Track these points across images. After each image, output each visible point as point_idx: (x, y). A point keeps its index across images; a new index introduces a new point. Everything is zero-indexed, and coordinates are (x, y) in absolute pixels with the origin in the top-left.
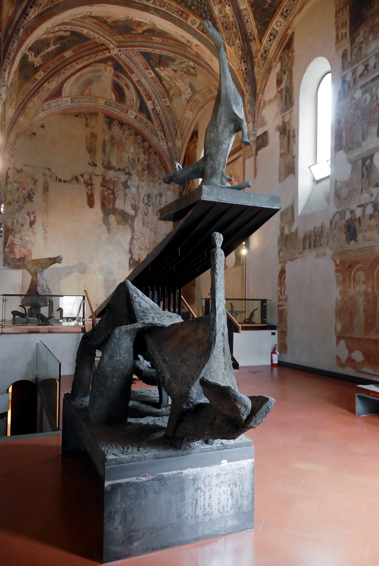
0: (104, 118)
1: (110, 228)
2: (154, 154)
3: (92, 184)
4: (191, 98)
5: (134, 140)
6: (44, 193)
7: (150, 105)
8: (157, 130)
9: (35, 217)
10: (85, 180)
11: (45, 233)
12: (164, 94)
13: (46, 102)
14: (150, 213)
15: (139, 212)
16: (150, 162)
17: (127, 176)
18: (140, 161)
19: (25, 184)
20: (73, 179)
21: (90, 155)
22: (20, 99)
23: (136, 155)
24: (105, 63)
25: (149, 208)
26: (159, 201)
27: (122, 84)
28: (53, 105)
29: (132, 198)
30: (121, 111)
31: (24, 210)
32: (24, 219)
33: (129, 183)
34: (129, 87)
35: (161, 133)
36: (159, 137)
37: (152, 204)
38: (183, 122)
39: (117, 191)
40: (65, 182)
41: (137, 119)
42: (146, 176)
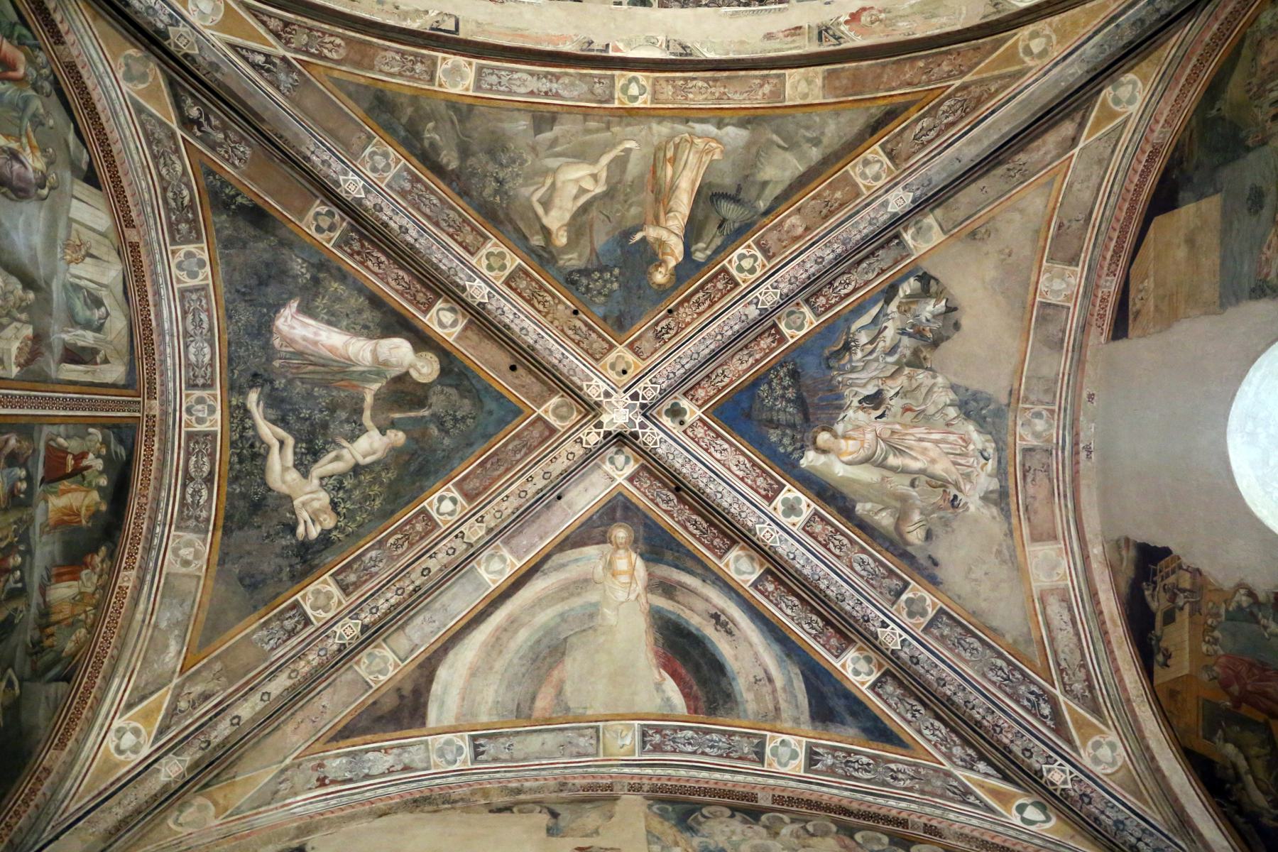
0: (650, 807)
4: (1001, 472)
7: (857, 673)
8: (948, 766)
12: (891, 572)
13: (341, 744)
22: (206, 697)
24: (603, 539)
27: (697, 621)
30: (728, 757)
34: (730, 625)
36: (977, 798)
38: (1048, 625)
41: (819, 766)
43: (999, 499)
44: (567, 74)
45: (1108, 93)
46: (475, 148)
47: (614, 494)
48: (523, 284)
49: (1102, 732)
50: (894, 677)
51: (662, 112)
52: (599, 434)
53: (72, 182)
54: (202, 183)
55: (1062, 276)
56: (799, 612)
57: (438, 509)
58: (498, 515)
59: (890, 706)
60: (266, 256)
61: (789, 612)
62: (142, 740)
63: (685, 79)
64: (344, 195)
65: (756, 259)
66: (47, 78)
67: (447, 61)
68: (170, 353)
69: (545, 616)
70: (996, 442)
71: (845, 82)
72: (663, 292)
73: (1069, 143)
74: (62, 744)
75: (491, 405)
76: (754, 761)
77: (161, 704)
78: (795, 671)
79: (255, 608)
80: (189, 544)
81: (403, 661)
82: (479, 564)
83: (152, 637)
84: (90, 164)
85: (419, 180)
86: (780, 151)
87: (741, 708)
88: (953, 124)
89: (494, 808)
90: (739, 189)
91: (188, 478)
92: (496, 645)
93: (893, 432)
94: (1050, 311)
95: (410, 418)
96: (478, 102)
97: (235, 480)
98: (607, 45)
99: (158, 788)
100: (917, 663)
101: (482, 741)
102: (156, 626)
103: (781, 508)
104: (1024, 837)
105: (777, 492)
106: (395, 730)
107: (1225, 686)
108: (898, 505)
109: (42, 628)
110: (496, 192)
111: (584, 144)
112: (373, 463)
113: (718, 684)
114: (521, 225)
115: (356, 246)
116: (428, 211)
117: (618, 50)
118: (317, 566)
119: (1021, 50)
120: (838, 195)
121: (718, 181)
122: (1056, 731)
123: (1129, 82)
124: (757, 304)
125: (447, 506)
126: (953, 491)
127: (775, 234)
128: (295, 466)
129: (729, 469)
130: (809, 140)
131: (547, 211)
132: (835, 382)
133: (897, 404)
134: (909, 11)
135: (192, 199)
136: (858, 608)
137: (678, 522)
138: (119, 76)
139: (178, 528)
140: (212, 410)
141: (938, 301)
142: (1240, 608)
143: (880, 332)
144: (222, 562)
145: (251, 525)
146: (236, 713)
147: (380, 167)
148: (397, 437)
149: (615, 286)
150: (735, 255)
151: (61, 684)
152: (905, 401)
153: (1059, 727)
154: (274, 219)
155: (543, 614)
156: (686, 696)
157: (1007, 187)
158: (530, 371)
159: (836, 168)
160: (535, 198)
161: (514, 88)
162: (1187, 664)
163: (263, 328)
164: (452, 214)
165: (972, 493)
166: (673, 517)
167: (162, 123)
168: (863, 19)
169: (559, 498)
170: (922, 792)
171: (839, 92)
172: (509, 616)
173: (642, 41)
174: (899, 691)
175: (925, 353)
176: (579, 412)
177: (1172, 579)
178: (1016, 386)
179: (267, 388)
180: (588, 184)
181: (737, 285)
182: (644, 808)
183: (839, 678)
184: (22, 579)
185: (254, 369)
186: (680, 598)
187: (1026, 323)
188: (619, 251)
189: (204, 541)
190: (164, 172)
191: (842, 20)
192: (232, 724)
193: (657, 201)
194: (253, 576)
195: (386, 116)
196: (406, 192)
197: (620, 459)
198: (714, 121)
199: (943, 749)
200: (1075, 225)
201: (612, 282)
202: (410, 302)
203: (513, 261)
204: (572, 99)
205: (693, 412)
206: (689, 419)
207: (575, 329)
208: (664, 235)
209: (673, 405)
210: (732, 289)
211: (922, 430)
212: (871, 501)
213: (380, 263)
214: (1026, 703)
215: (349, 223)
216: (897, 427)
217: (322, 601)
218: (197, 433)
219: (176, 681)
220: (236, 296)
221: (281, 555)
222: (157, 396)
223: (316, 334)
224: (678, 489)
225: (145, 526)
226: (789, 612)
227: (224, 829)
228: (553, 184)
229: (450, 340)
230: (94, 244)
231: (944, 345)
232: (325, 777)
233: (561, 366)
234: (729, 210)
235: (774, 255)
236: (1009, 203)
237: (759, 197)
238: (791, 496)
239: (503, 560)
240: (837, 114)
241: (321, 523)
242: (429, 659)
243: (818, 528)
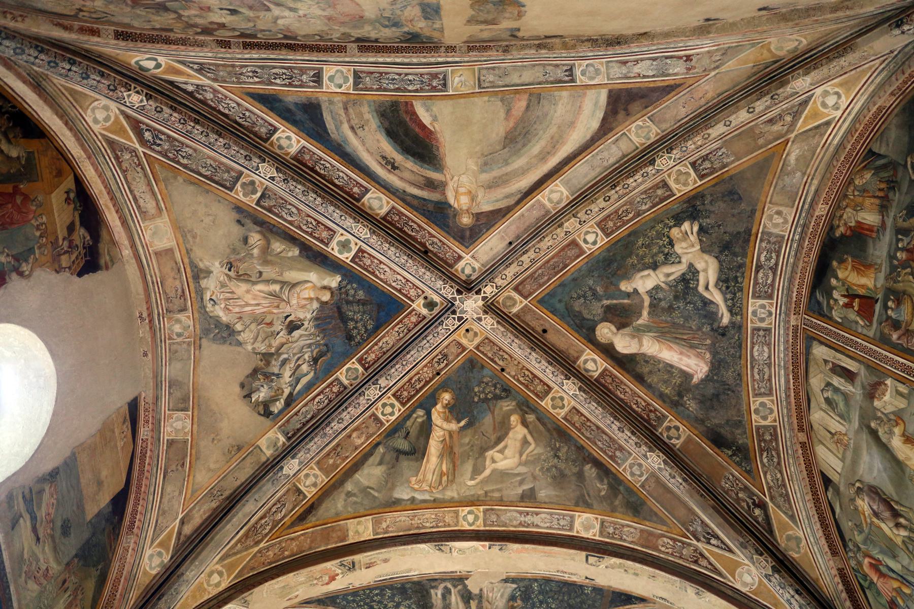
4: (200, 292)
8: (216, 85)
12: (270, 211)
13: (673, 83)
22: (771, 121)
24: (478, 216)
27: (408, 164)
28: (644, 68)
30: (381, 73)
38: (154, 194)
43: (198, 274)
44: (515, 527)
45: (166, 558)
46: (574, 478)
47: (471, 247)
48: (539, 388)
49: (104, 129)
50: (261, 138)
51: (451, 505)
52: (485, 293)
53: (839, 483)
54: (754, 466)
55: (177, 431)
56: (334, 175)
57: (597, 236)
58: (555, 236)
59: (262, 119)
60: (713, 414)
61: (341, 174)
62: (821, 99)
63: (437, 527)
64: (661, 454)
66: (850, 550)
67: (593, 534)
68: (781, 354)
69: (519, 163)
70: (206, 312)
71: (334, 535)
72: (444, 386)
73: (185, 520)
75: (560, 307)
76: (361, 72)
77: (804, 122)
78: (334, 135)
79: (731, 178)
80: (776, 225)
81: (624, 133)
82: (567, 197)
83: (808, 167)
84: (827, 489)
85: (611, 457)
86: (372, 486)
87: (373, 108)
88: (261, 518)
90: (397, 459)
91: (774, 269)
92: (555, 143)
93: (278, 307)
94: (182, 406)
95: (616, 299)
96: (573, 508)
97: (741, 266)
98: (490, 548)
99: (813, 73)
100: (246, 157)
101: (567, 79)
102: (804, 174)
103: (352, 245)
105: (355, 256)
106: (631, 89)
107: (26, 198)
108: (269, 258)
109: (885, 198)
110: (558, 449)
111: (502, 482)
112: (643, 270)
113: (391, 123)
114: (541, 427)
115: (652, 416)
116: (604, 437)
117: (483, 546)
118: (685, 203)
119: (225, 573)
120: (331, 461)
121: (411, 463)
122: (138, 122)
123: (154, 568)
124: (380, 388)
125: (591, 238)
126: (232, 274)
127: (371, 431)
128: (698, 272)
129: (391, 269)
130: (354, 495)
131: (525, 437)
132: (321, 335)
133: (278, 327)
134: (298, 587)
135: (761, 455)
136: (292, 187)
137: (425, 230)
138: (804, 541)
139: (783, 237)
140: (754, 313)
141: (257, 400)
142: (26, 261)
143: (294, 373)
144: (753, 212)
145: (731, 234)
146: (751, 115)
147: (636, 467)
148: (625, 286)
149: (476, 389)
150: (397, 415)
151: (877, 151)
152: (272, 329)
153: (136, 126)
154: (708, 439)
155: (521, 164)
156: (414, 113)
157: (221, 483)
158: (533, 329)
159: (334, 479)
161: (548, 517)
162: (54, 201)
163: (717, 366)
164: (588, 435)
165: (219, 275)
166: (429, 232)
167: (779, 507)
168: (327, 578)
169: (510, 243)
170: (233, 66)
171: (337, 528)
173: (467, 551)
174: (257, 129)
175: (262, 364)
176: (498, 302)
177: (73, 257)
178: (197, 352)
179: (715, 326)
180: (498, 456)
181: (394, 395)
183: (301, 134)
184: (898, 240)
185: (724, 339)
186: (421, 179)
187: (196, 395)
188: (475, 413)
189: (765, 227)
190: (779, 475)
191: (341, 576)
192: (754, 108)
193: (451, 448)
194: (732, 200)
195: (632, 499)
196: (619, 450)
197: (468, 271)
198: (417, 502)
199: (220, 96)
200: (173, 467)
201: (479, 391)
202: (616, 377)
203: (546, 403)
204: (511, 511)
205: (419, 306)
206: (421, 301)
207: (503, 359)
208: (445, 425)
209: (432, 310)
210: (397, 392)
211: (258, 312)
212: (289, 258)
213: (637, 404)
214: (163, 137)
215: (657, 431)
216: (275, 311)
218: (765, 298)
219: (793, 135)
220: (734, 389)
221: (710, 212)
222: (791, 328)
223: (681, 359)
224: (426, 252)
225: (807, 243)
226: (341, 174)
227: (764, 35)
228: (521, 455)
229: (588, 351)
230: (828, 439)
231: (249, 371)
232: (686, 61)
233: (512, 338)
234: (403, 445)
235: (370, 417)
236: (218, 474)
237: (384, 454)
238: (346, 255)
239: (550, 200)
240: (337, 514)
241: (681, 231)
242: (605, 134)
243: (325, 234)
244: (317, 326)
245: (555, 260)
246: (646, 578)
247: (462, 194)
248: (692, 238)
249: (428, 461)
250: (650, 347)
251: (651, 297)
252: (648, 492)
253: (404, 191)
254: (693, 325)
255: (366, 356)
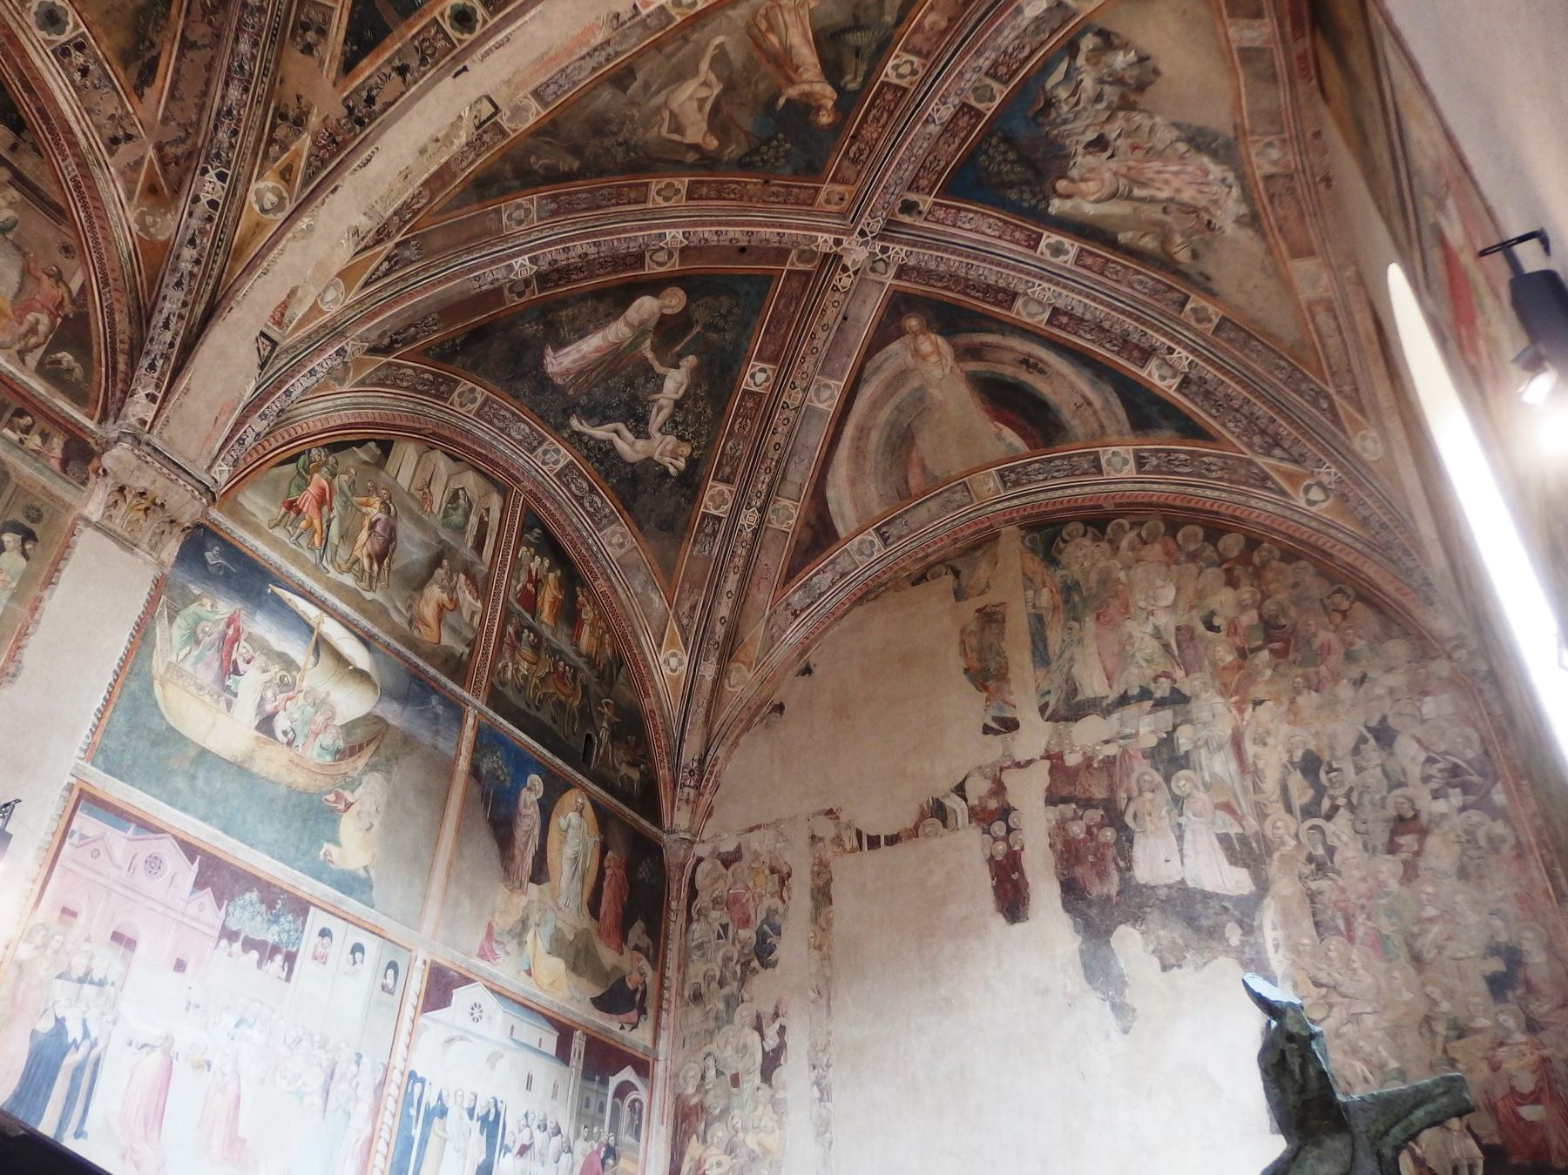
1: (1127, 1000)
2: (1283, 565)
3: (1005, 812)
4: (1247, 196)
5: (1168, 554)
6: (815, 920)
7: (1163, 378)
9: (782, 1029)
10: (977, 802)
11: (821, 1100)
12: (1171, 288)
14: (1349, 851)
15: (1274, 867)
16: (1270, 607)
17: (1166, 715)
18: (1217, 621)
19: (748, 900)
20: (923, 816)
21: (986, 694)
22: (693, 608)
23: (1192, 608)
24: (901, 333)
25: (1329, 827)
26: (1385, 773)
27: (1009, 371)
29: (1219, 806)
30: (1073, 475)
31: (744, 1013)
32: (743, 1050)
33: (1184, 739)
35: (1274, 457)
36: (1274, 482)
37: (1341, 801)
38: (1318, 331)
39: (1129, 799)
40: (893, 840)
41: (1147, 467)
42: (1268, 673)
54: (429, 360)
59: (1196, 404)
65: (912, 63)
69: (884, 415)
72: (836, 128)
74: (647, 695)
78: (1109, 390)
79: (682, 538)
80: (614, 534)
89: (913, 579)
90: (856, 17)
91: (579, 499)
92: (858, 451)
93: (1129, 168)
98: (635, 6)
101: (884, 529)
102: (636, 594)
104: (1305, 520)
108: (1158, 230)
110: (627, 152)
114: (669, 157)
124: (934, 121)
125: (760, 377)
128: (637, 438)
129: (983, 233)
132: (1051, 136)
133: (1123, 144)
137: (959, 292)
139: (600, 531)
140: (557, 451)
144: (641, 528)
148: (690, 361)
152: (1130, 141)
156: (1024, 437)
160: (664, 131)
161: (576, 78)
163: (544, 382)
164: (605, 192)
166: (952, 291)
167: (377, 370)
170: (1231, 482)
172: (857, 426)
180: (703, 93)
182: (1019, 542)
183: (1147, 385)
190: (405, 384)
199: (1245, 439)
203: (683, 183)
205: (926, 202)
206: (924, 208)
208: (806, 88)
217: (718, 500)
226: (1089, 336)
228: (672, 113)
231: (1151, 90)
234: (854, 39)
237: (881, 14)
242: (815, 489)
243: (1089, 261)
244: (1063, 147)
245: (783, 331)
246: (410, 161)
247: (932, 353)
248: (668, 459)
249: (805, 35)
250: (617, 331)
251: (658, 375)
252: (488, 213)
253: (1003, 334)
254: (598, 392)
255: (973, 121)
